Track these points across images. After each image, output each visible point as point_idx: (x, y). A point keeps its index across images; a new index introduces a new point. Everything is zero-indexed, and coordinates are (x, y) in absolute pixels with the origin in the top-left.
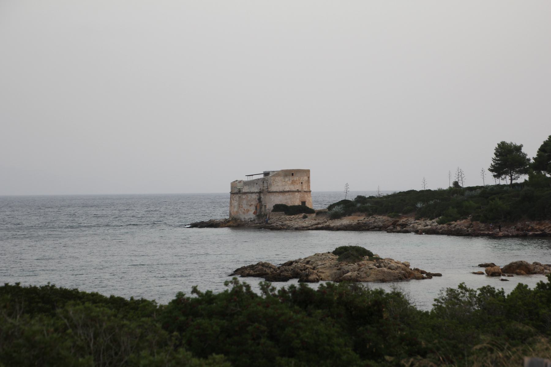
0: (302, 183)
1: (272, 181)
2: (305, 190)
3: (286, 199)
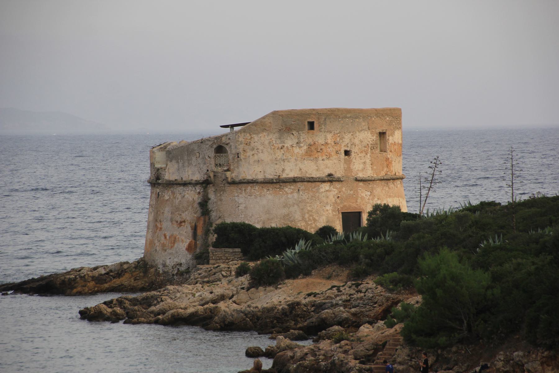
0: (347, 153)
1: (241, 147)
2: (361, 175)
3: (285, 206)
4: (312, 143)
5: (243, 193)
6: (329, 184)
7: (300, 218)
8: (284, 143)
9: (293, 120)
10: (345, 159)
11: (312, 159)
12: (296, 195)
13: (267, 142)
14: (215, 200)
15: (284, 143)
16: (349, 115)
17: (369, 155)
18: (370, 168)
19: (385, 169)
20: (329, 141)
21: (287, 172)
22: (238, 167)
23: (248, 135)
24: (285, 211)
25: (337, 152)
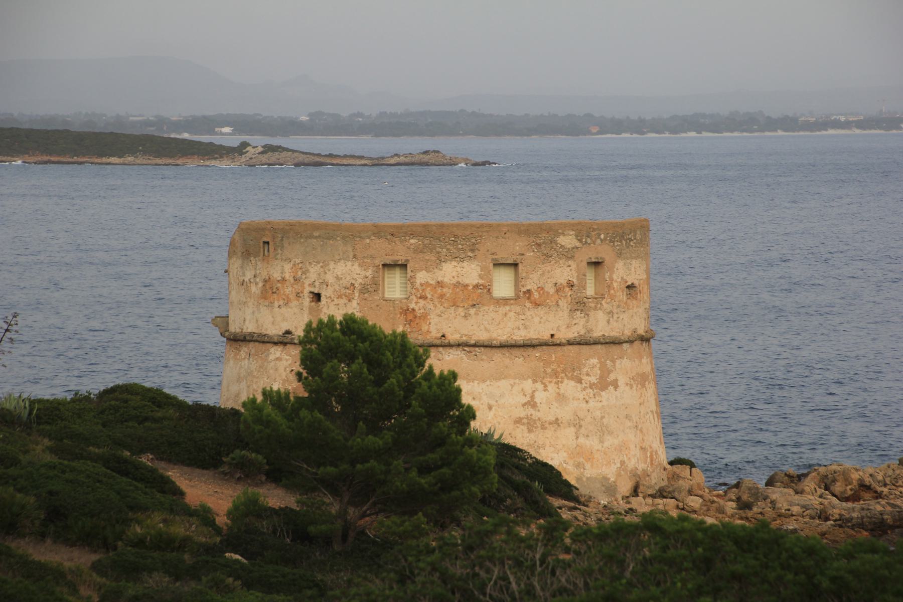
10: (310, 308)
12: (246, 361)
16: (316, 234)
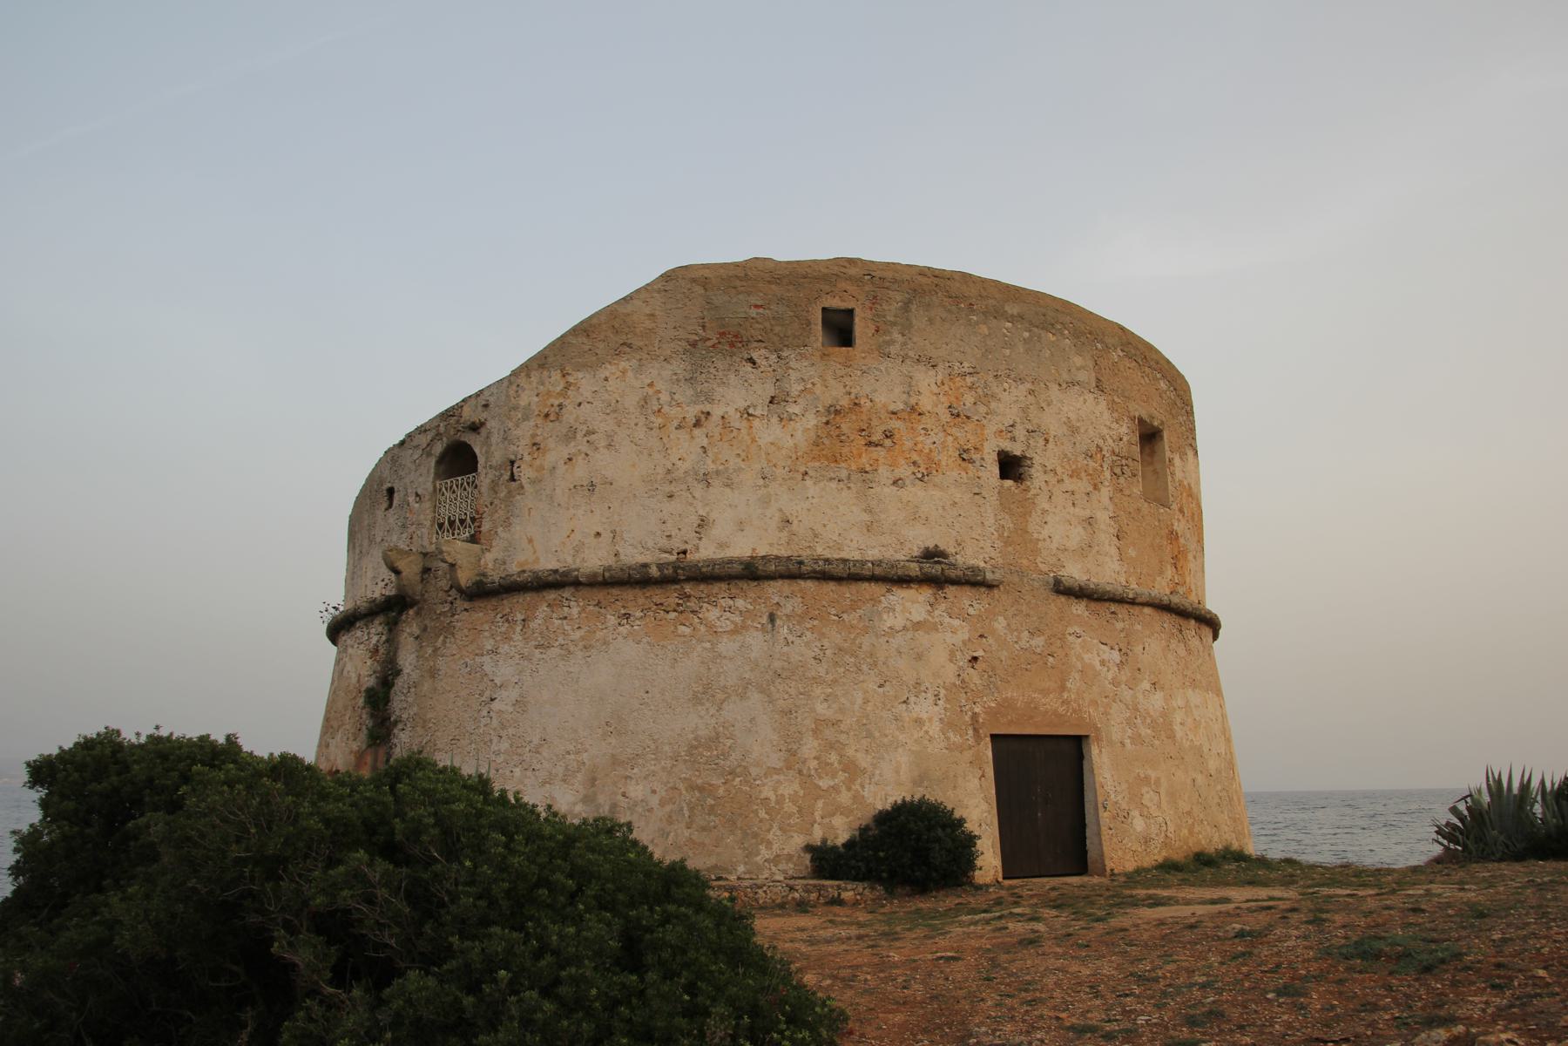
0: (1011, 466)
1: (524, 433)
2: (1075, 573)
3: (705, 693)
4: (845, 402)
5: (517, 637)
6: (926, 593)
7: (776, 760)
8: (709, 399)
9: (754, 300)
11: (844, 474)
12: (756, 641)
13: (631, 401)
14: (415, 676)
15: (709, 399)
17: (1105, 492)
18: (1114, 551)
19: (1169, 572)
20: (926, 403)
21: (719, 531)
22: (507, 523)
23: (556, 375)
24: (696, 722)
25: (964, 457)
